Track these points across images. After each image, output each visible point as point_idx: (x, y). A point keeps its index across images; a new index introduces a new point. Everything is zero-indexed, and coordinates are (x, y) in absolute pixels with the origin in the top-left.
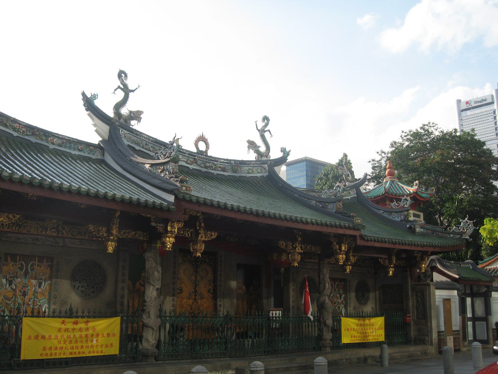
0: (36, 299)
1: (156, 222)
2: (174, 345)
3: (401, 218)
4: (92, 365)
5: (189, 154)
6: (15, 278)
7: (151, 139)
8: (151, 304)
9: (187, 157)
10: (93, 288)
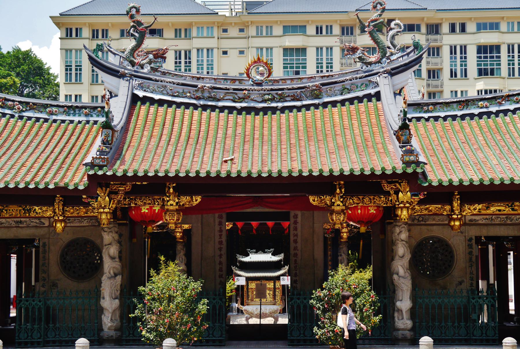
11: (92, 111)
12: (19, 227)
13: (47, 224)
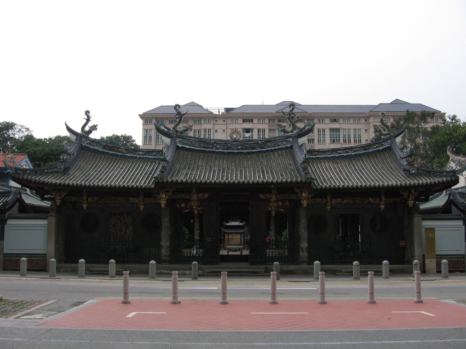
9: (223, 145)
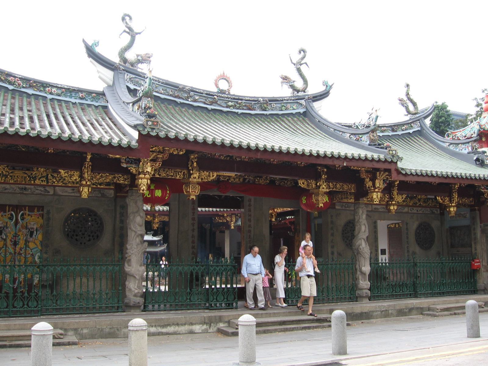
0: (27, 249)
1: (127, 163)
2: (215, 294)
3: (469, 150)
4: (74, 314)
5: (207, 94)
6: (5, 228)
7: (161, 81)
8: (132, 251)
9: (205, 97)
10: (89, 236)
11: (87, 96)
12: (23, 193)
13: (52, 192)
